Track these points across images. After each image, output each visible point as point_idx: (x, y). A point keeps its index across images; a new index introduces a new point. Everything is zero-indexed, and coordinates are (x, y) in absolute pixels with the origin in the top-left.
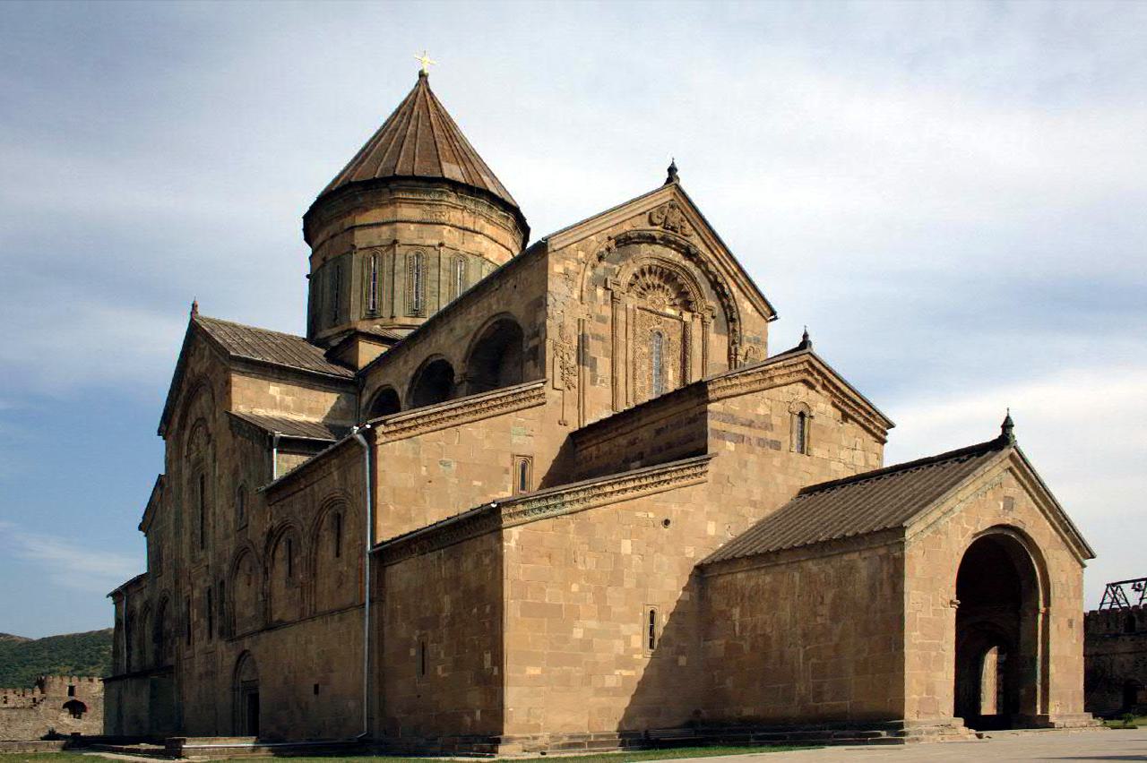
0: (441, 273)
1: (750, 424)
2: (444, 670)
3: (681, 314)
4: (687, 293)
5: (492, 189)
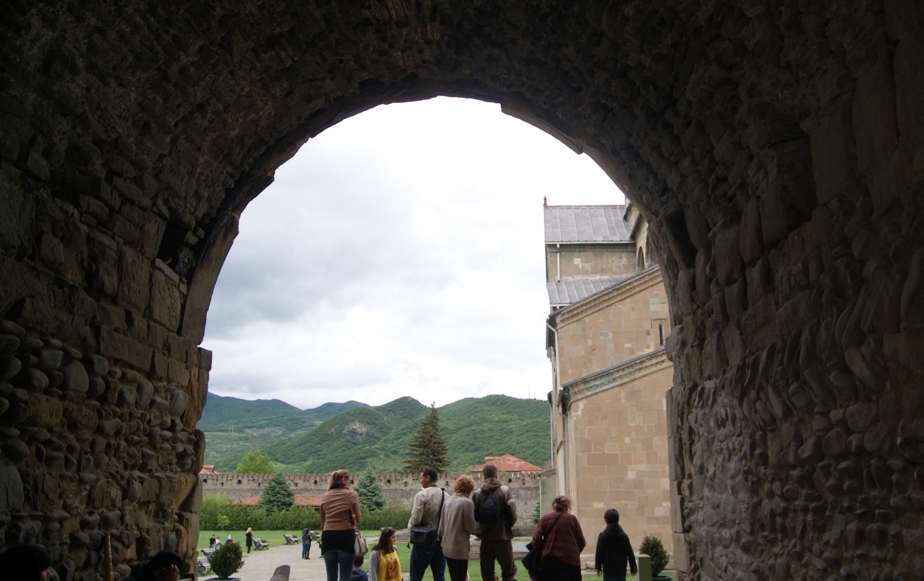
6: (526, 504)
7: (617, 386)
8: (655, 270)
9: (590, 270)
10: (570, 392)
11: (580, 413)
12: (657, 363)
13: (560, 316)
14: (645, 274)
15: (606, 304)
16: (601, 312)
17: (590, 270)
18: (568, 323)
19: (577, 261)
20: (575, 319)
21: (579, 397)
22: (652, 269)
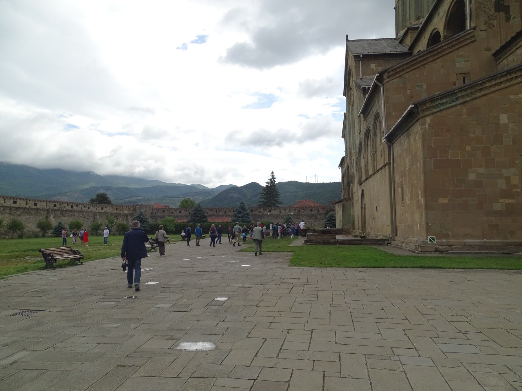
2: (408, 200)
6: (320, 222)
7: (460, 104)
8: (461, 36)
10: (419, 109)
11: (427, 126)
12: (495, 85)
13: (386, 73)
14: (453, 40)
16: (418, 70)
18: (392, 78)
19: (373, 66)
21: (427, 113)
22: (459, 35)
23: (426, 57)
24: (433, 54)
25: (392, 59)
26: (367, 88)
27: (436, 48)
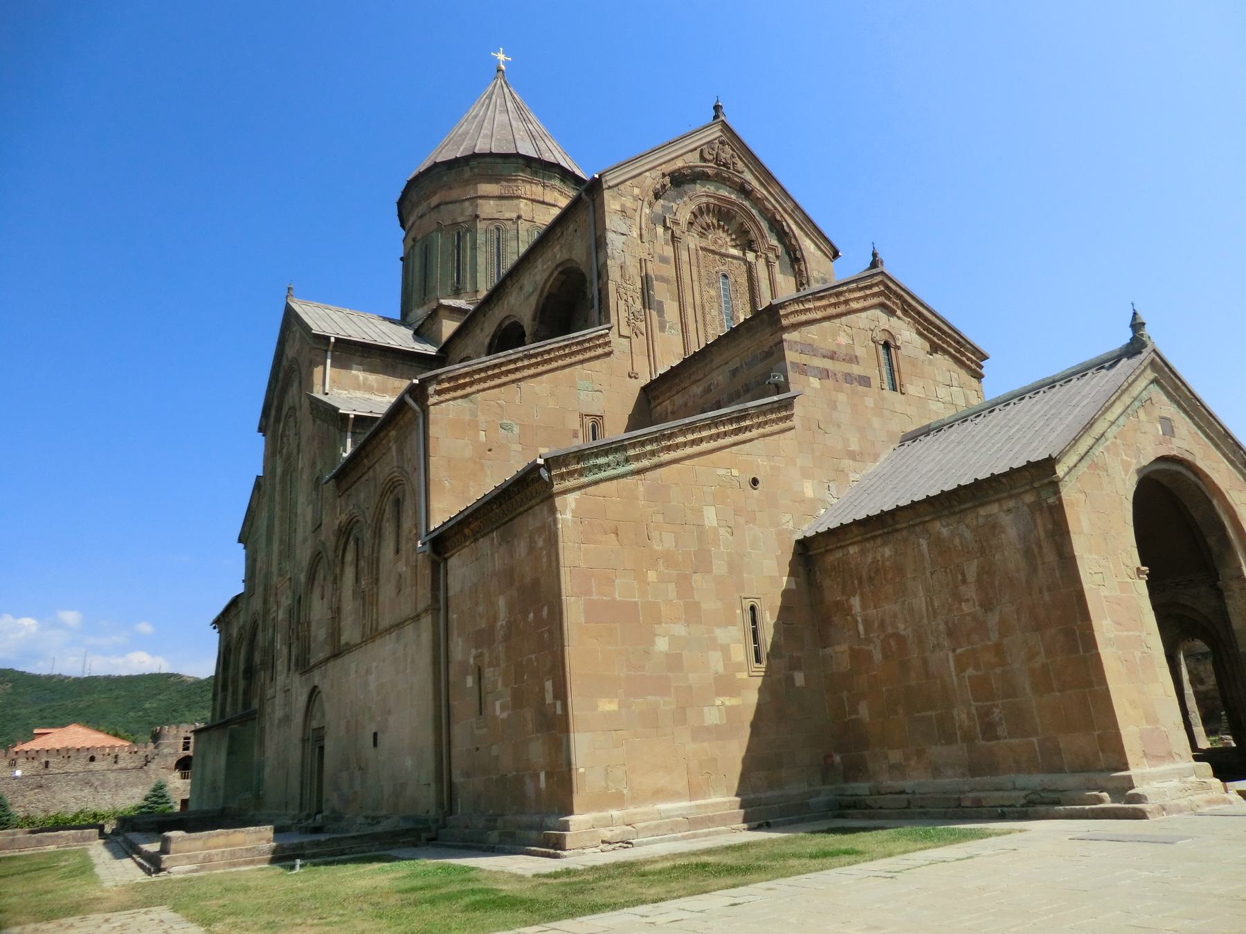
0: (520, 245)
1: (832, 356)
2: (503, 708)
3: (744, 254)
4: (747, 232)
5: (563, 164)
8: (588, 337)
9: (375, 385)
10: (553, 473)
11: (568, 516)
15: (512, 377)
17: (375, 385)
18: (448, 396)
20: (460, 393)
22: (584, 335)
23: (520, 364)
24: (534, 360)
25: (403, 363)
26: (352, 416)
27: (541, 350)
